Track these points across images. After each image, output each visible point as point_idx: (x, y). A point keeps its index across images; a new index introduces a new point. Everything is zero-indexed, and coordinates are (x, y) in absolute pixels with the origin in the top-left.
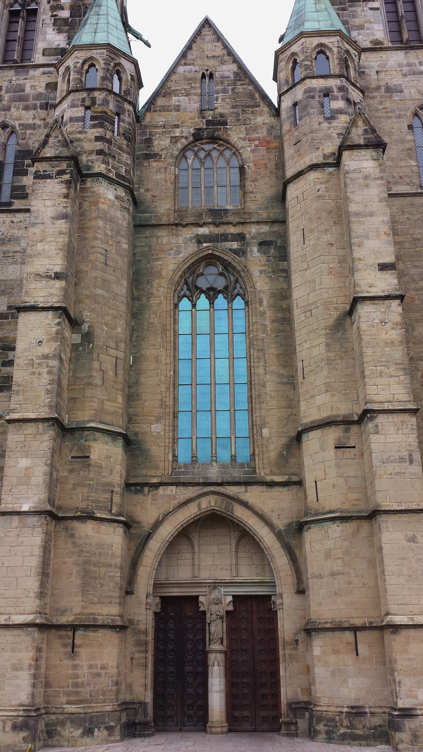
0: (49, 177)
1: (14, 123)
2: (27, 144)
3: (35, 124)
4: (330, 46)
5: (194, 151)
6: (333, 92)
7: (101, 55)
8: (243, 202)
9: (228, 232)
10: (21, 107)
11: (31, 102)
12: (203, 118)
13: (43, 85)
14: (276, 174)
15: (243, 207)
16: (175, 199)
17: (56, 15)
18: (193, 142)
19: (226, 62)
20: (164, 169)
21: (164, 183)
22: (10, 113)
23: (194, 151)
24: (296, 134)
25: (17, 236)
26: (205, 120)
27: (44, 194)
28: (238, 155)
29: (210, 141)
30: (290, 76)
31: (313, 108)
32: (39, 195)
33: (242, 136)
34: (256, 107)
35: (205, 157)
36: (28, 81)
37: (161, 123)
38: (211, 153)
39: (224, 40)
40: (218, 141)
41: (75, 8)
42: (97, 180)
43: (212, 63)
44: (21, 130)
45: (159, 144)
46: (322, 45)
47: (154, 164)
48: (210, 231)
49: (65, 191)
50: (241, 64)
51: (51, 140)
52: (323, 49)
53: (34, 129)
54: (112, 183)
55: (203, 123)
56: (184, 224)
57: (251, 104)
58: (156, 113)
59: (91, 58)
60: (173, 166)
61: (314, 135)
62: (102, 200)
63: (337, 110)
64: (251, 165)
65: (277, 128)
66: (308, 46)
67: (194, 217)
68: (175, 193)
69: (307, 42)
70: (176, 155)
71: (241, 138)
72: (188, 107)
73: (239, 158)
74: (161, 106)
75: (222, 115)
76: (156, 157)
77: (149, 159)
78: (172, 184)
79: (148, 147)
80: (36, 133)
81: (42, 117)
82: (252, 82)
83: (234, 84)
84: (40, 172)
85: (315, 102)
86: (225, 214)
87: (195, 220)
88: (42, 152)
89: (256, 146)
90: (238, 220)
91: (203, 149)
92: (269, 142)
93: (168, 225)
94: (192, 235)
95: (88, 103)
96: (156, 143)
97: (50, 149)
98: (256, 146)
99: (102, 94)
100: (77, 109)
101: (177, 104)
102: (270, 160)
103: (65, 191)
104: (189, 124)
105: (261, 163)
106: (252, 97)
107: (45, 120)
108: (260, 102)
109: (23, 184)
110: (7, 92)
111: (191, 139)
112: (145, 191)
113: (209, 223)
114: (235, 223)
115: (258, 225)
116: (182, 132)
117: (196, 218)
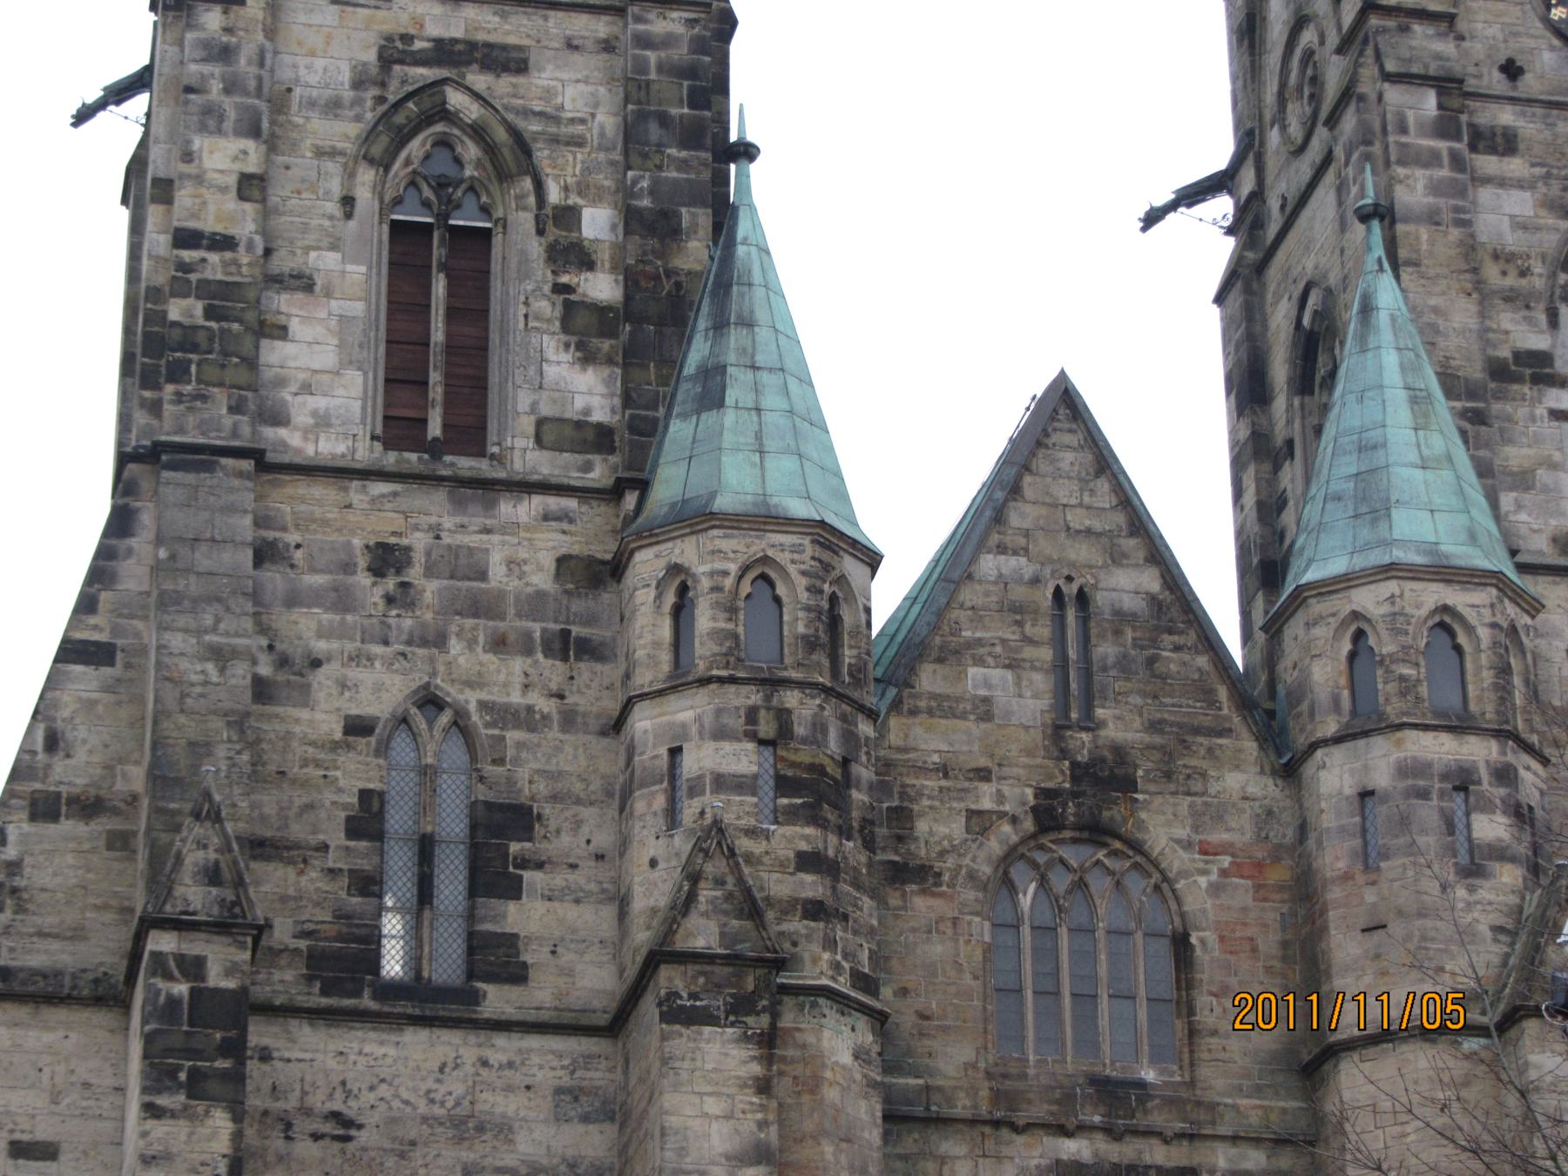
0: (707, 1018)
1: (461, 697)
2: (511, 782)
3: (530, 709)
4: (1470, 619)
5: (1034, 865)
6: (1479, 783)
7: (796, 556)
8: (1186, 1061)
9: (1148, 1159)
10: (481, 639)
11: (512, 624)
12: (1064, 753)
13: (548, 561)
14: (1285, 977)
15: (1187, 1078)
16: (985, 1031)
17: (567, 289)
18: (1034, 836)
19: (1125, 555)
20: (949, 924)
21: (952, 973)
22: (442, 658)
23: (1034, 865)
24: (1370, 896)
25: (504, 1115)
26: (1067, 763)
27: (697, 1073)
28: (1169, 894)
29: (1086, 835)
30: (1343, 681)
31: (1423, 832)
32: (684, 1075)
33: (1182, 833)
34: (1220, 734)
35: (1069, 892)
36: (496, 538)
37: (936, 758)
38: (1089, 878)
39: (1121, 478)
40: (1109, 840)
41: (643, 283)
42: (814, 1005)
43: (1082, 552)
44: (488, 725)
45: (931, 833)
46: (1445, 609)
47: (920, 903)
48: (1096, 1154)
49: (756, 1069)
50: (1175, 571)
51: (706, 894)
52: (1447, 619)
53: (532, 728)
54: (846, 1010)
55: (1062, 772)
56: (1021, 1123)
57: (1207, 721)
58: (918, 720)
59: (765, 560)
60: (977, 914)
61: (1428, 923)
62: (828, 1074)
63: (1489, 845)
64: (1210, 936)
65: (1286, 817)
66: (1408, 610)
67: (1051, 1102)
68: (985, 1008)
69: (1407, 594)
70: (984, 878)
71: (1178, 842)
72: (1015, 708)
73: (1174, 906)
74: (933, 696)
75: (1120, 752)
76: (923, 880)
77: (904, 882)
78: (976, 978)
79: (900, 839)
80: (539, 745)
81: (554, 687)
82: (1159, 556)
83: (1154, 643)
84: (681, 998)
85: (1428, 813)
86: (1142, 1100)
87: (1052, 1114)
88: (681, 931)
89: (1224, 873)
90: (1179, 1126)
91: (1062, 861)
92: (1259, 866)
93: (973, 1122)
94: (1043, 1162)
95: (766, 728)
96: (922, 826)
97: (702, 921)
98: (1224, 873)
99: (808, 701)
100: (737, 746)
101: (982, 692)
102: (1265, 926)
103: (756, 1069)
104: (1021, 771)
105: (1238, 934)
106: (1211, 700)
107: (561, 697)
108: (1229, 719)
109: (508, 930)
110: (430, 572)
111: (1029, 825)
112: (895, 994)
113: (1092, 1128)
114: (1170, 1133)
115: (1235, 1145)
116: (1000, 798)
117: (1054, 1108)
